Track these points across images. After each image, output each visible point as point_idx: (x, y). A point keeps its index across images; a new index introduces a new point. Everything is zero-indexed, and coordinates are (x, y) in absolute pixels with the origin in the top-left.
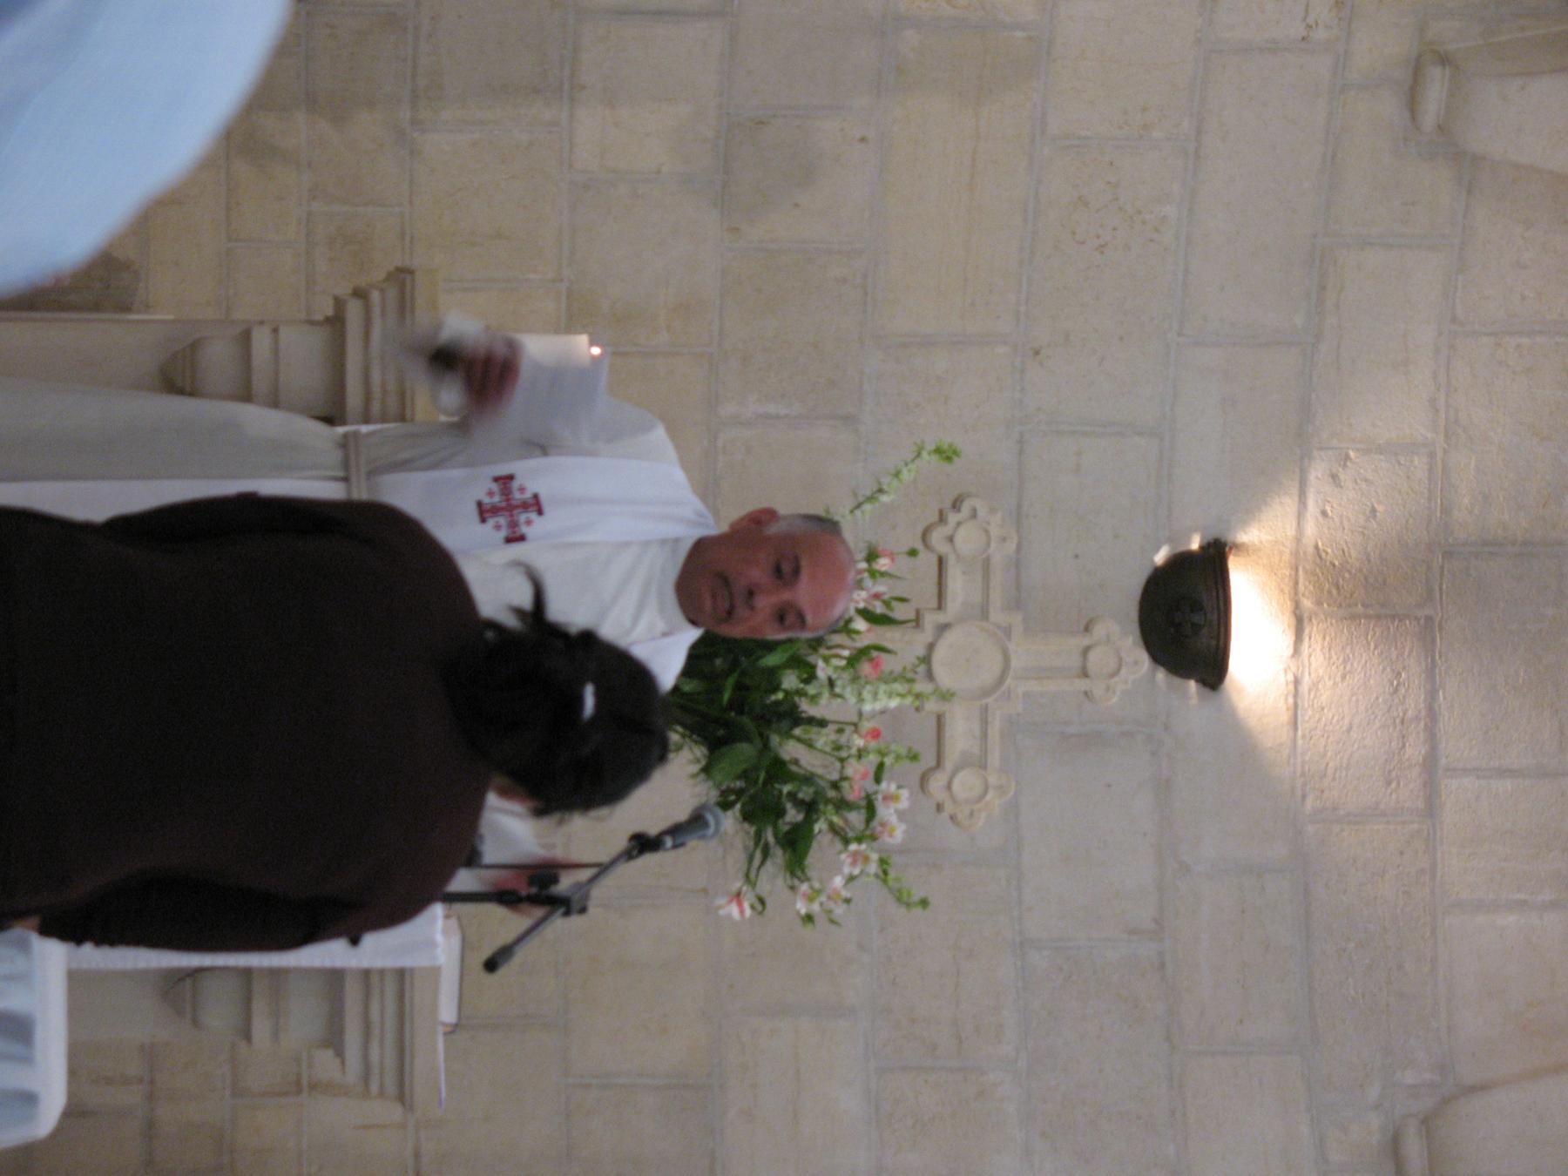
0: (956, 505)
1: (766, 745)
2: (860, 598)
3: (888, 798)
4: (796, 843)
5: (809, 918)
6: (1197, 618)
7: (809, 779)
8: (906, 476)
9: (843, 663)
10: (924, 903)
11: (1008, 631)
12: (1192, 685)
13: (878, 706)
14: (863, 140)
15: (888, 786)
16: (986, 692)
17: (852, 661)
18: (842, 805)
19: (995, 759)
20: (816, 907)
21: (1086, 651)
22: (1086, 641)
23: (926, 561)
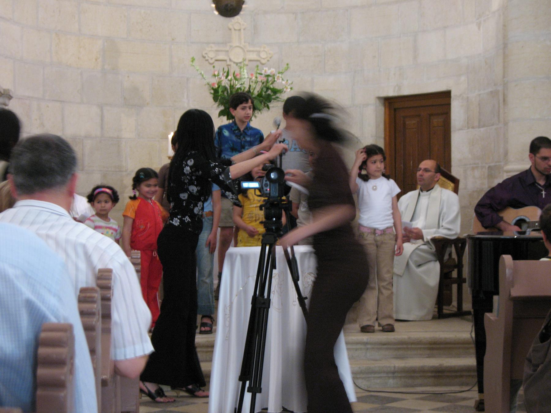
0: (204, 57)
1: (255, 98)
2: (223, 78)
3: (265, 72)
4: (275, 91)
5: (291, 88)
6: (229, 5)
7: (262, 89)
8: (198, 68)
9: (237, 82)
10: (288, 64)
11: (231, 46)
12: (244, 6)
13: (246, 74)
14: (128, 77)
15: (263, 72)
16: (244, 51)
17: (236, 79)
18: (267, 82)
19: (258, 49)
20: (289, 87)
21: (235, 30)
23: (216, 64)
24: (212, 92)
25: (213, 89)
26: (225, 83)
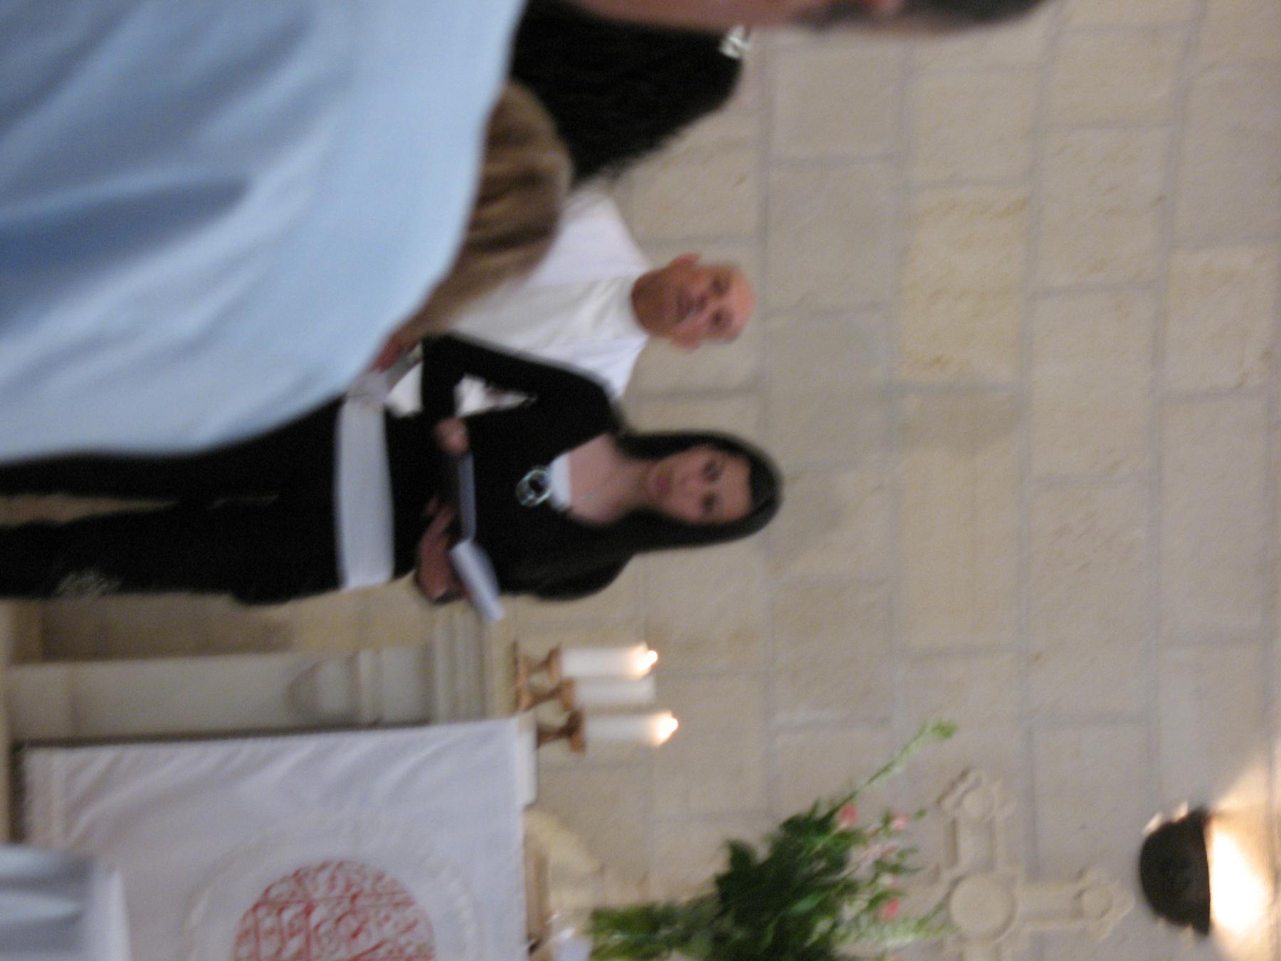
0: (964, 775)
17: (874, 902)
21: (1080, 894)
22: (1080, 885)
24: (822, 812)
25: (830, 815)
26: (861, 860)
